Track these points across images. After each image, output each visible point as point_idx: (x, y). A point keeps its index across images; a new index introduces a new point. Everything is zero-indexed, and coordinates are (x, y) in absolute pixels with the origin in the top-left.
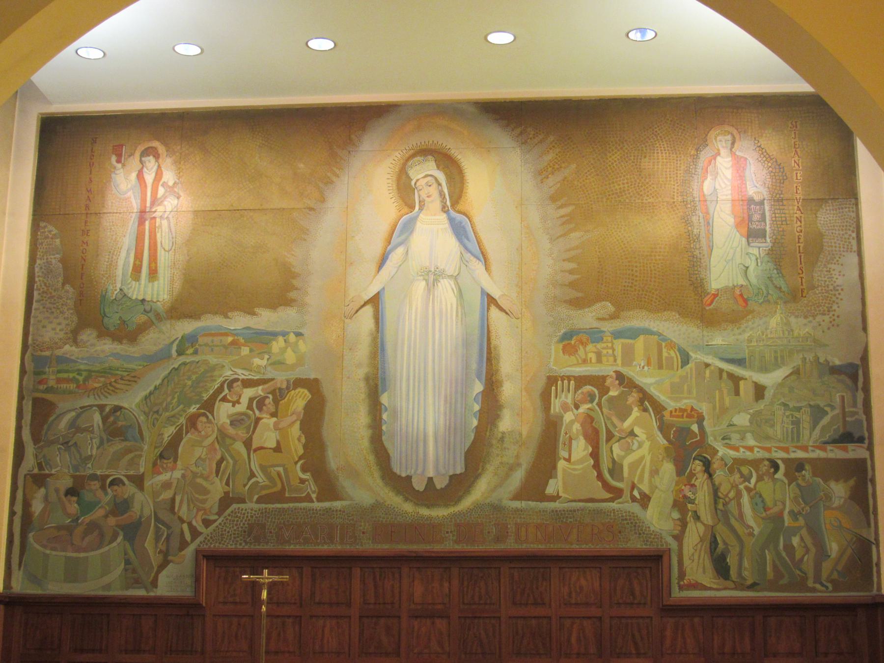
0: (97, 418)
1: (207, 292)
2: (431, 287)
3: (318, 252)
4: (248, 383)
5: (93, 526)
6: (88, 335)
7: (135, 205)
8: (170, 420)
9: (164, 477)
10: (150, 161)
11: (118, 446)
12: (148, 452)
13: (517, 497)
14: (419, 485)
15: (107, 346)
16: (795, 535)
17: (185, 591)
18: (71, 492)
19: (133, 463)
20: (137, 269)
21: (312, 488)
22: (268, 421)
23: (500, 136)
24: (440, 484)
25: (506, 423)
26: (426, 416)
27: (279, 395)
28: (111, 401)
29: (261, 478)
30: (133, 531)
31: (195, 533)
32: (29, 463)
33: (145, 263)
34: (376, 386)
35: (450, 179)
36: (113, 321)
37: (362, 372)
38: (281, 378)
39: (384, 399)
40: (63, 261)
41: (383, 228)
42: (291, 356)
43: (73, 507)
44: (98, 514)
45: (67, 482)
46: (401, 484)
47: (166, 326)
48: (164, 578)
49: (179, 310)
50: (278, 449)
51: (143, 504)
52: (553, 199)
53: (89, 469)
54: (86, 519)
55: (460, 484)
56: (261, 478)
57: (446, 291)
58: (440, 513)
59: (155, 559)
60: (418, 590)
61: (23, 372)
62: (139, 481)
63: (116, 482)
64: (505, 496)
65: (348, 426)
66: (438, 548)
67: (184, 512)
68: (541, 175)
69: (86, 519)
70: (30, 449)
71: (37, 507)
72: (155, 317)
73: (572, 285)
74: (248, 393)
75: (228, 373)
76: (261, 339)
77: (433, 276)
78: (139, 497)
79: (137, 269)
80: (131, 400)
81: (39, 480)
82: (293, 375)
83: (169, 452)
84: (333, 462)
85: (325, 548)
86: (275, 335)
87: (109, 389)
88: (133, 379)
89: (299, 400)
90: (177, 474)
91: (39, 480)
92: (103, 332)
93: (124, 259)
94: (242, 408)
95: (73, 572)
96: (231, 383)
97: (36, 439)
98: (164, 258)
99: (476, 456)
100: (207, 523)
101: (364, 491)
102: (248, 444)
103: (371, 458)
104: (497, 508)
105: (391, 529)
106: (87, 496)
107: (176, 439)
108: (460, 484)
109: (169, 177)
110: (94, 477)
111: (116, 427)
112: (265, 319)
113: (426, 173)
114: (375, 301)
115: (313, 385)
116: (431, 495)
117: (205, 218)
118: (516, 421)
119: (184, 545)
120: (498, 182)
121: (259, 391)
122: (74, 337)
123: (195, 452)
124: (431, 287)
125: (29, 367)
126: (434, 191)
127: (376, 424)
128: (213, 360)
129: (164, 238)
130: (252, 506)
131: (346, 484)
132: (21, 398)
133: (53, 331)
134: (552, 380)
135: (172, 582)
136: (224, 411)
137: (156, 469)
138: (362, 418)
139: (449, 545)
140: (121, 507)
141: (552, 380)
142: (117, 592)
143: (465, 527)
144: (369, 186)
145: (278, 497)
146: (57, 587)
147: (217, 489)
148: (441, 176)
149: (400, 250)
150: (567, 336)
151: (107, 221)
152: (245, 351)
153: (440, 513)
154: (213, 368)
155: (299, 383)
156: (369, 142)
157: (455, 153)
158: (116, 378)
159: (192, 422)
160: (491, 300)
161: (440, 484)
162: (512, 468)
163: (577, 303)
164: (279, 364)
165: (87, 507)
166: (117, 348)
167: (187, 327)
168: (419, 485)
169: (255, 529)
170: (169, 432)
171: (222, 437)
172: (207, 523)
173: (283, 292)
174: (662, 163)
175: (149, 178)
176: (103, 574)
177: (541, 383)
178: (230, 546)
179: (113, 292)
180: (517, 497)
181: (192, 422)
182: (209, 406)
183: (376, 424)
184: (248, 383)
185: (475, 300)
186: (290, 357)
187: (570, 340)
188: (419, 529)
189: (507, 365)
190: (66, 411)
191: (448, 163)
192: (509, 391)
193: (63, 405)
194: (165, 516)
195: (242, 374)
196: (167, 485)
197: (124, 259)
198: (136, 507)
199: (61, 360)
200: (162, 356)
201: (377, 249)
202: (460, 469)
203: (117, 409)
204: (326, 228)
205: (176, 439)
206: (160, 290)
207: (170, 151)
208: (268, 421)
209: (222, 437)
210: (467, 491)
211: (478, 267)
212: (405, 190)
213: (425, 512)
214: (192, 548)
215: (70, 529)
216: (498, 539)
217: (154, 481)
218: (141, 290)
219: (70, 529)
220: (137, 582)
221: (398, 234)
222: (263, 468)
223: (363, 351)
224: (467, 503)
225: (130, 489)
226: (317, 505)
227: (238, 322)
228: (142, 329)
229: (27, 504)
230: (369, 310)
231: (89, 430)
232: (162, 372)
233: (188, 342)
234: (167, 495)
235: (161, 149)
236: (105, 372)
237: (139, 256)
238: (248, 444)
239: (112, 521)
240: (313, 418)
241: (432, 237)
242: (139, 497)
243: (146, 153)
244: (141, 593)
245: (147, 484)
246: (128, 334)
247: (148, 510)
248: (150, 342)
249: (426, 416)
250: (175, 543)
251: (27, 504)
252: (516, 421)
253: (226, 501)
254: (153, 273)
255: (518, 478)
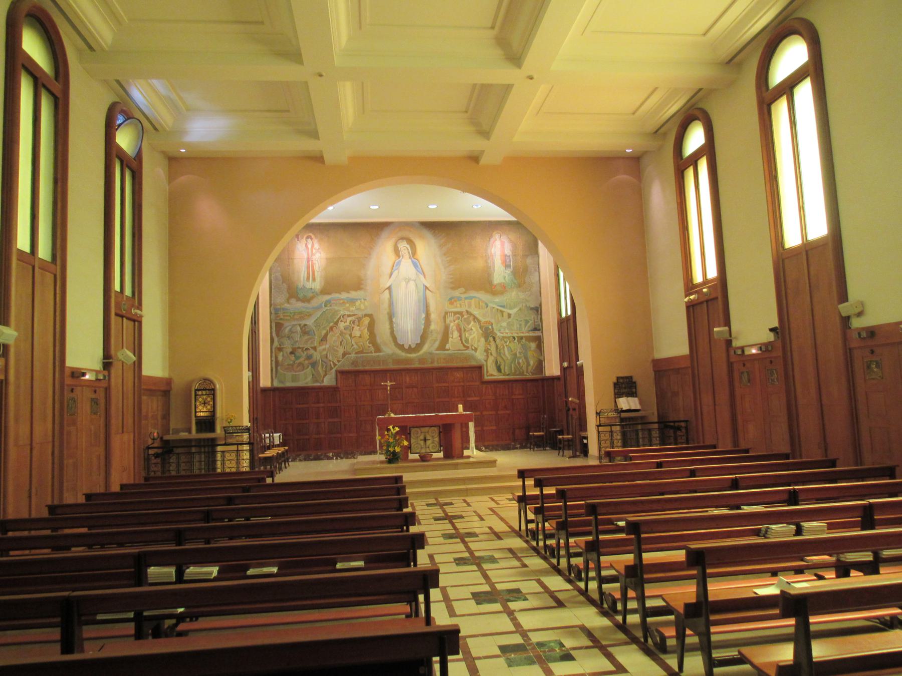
0: (299, 328)
1: (332, 286)
2: (407, 283)
3: (370, 272)
4: (349, 316)
5: (300, 364)
6: (293, 301)
7: (306, 256)
8: (324, 328)
9: (323, 347)
10: (309, 240)
11: (306, 337)
12: (317, 339)
13: (437, 350)
14: (406, 347)
15: (300, 305)
16: (641, 403)
17: (333, 383)
18: (291, 353)
19: (312, 343)
20: (308, 279)
21: (372, 349)
22: (356, 328)
23: (427, 234)
24: (413, 346)
25: (433, 327)
26: (408, 325)
27: (359, 319)
28: (303, 323)
29: (355, 346)
30: (314, 365)
31: (335, 365)
32: (276, 344)
33: (310, 276)
34: (391, 316)
35: (411, 247)
36: (301, 295)
37: (386, 312)
38: (360, 314)
39: (394, 320)
40: (282, 276)
41: (391, 264)
42: (363, 307)
43: (293, 358)
44: (301, 360)
45: (290, 350)
46: (401, 347)
47: (320, 297)
48: (326, 379)
49: (324, 291)
50: (360, 337)
51: (317, 356)
52: (445, 254)
53: (297, 345)
54: (298, 361)
55: (419, 346)
56: (355, 346)
57: (412, 285)
58: (413, 355)
59: (322, 373)
60: (408, 379)
61: (271, 313)
62: (315, 348)
63: (307, 349)
64: (433, 350)
65: (383, 329)
66: (413, 366)
67: (331, 358)
68: (441, 246)
69: (298, 361)
70: (276, 339)
71: (280, 358)
72: (315, 295)
73: (452, 283)
74: (349, 319)
75: (342, 313)
76: (352, 301)
77: (408, 281)
78: (315, 353)
79: (308, 279)
80: (310, 322)
81: (280, 349)
82: (364, 313)
83: (324, 339)
84: (379, 340)
85: (378, 368)
86: (357, 300)
87: (302, 318)
88: (310, 315)
89: (366, 321)
90: (327, 346)
91: (280, 349)
92: (298, 299)
93: (303, 274)
94: (348, 323)
95: (294, 379)
96: (343, 316)
97: (278, 335)
98: (317, 274)
99: (424, 338)
100: (339, 361)
101: (389, 349)
102: (350, 335)
103: (391, 339)
104: (431, 353)
105: (398, 361)
106: (297, 354)
107: (326, 335)
108: (419, 346)
109: (316, 246)
110: (299, 348)
111: (305, 331)
112: (353, 294)
113: (403, 246)
114: (389, 288)
115: (370, 316)
116: (410, 350)
117: (330, 261)
118: (436, 326)
119: (331, 369)
120: (427, 248)
121: (353, 318)
122: (288, 302)
123: (333, 338)
124: (407, 283)
125: (273, 312)
126: (406, 251)
127: (392, 328)
128: (336, 308)
129: (317, 268)
130: (353, 355)
131: (383, 347)
132: (271, 322)
133: (280, 300)
134: (446, 313)
135: (329, 380)
136: (342, 325)
137: (320, 344)
138: (387, 326)
139: (417, 365)
140: (309, 357)
141: (446, 313)
142: (310, 384)
143: (421, 360)
144: (384, 251)
145: (362, 352)
146: (289, 384)
147: (341, 351)
148: (408, 246)
149: (396, 272)
150: (451, 299)
151: (295, 261)
152: (347, 305)
153: (413, 355)
154: (337, 311)
155: (366, 315)
156: (385, 234)
157: (413, 239)
158: (303, 315)
159: (331, 329)
160: (426, 288)
161: (413, 346)
162: (435, 341)
163: (453, 288)
164: (358, 309)
165: (297, 358)
166: (303, 305)
167: (327, 298)
168: (406, 347)
169: (354, 363)
170: (324, 332)
171: (342, 333)
172: (339, 361)
173: (358, 285)
174: (478, 242)
175: (310, 247)
176: (305, 379)
177: (443, 314)
178: (347, 368)
179: (300, 286)
180: (437, 350)
181: (331, 329)
182: (336, 323)
183: (392, 328)
184: (349, 316)
185: (422, 288)
186: (362, 307)
187: (452, 301)
188: (407, 361)
189: (432, 308)
190: (287, 327)
191: (410, 242)
192: (433, 316)
193: (286, 324)
194: (325, 360)
195: (347, 313)
196: (324, 350)
197: (303, 274)
198: (314, 357)
199: (283, 309)
200: (319, 308)
201: (389, 271)
202: (419, 342)
203: (305, 325)
204: (372, 263)
205: (326, 335)
206: (317, 285)
207: (316, 237)
208: (356, 328)
209: (342, 333)
210: (421, 349)
211: (422, 277)
212: (397, 252)
213: (409, 355)
214: (334, 370)
215: (292, 365)
216: (432, 363)
217: (320, 348)
218: (310, 285)
219: (292, 365)
220: (317, 381)
221: (395, 267)
222: (356, 343)
223: (386, 305)
224: (421, 352)
225: (312, 351)
226: (374, 354)
227: (344, 295)
228: (312, 298)
229: (276, 358)
230: (387, 291)
231: (296, 332)
232: (319, 314)
233: (327, 303)
234: (325, 353)
235: (313, 236)
236: (300, 313)
237: (308, 273)
238: (350, 335)
239: (307, 362)
240: (371, 327)
241: (406, 267)
242: (315, 353)
243: (307, 238)
244: (318, 384)
245: (318, 349)
246: (307, 300)
247: (319, 358)
248: (315, 303)
249: (408, 325)
250: (328, 368)
251: (276, 358)
252: (436, 326)
253: (344, 354)
254: (314, 279)
255: (437, 343)
